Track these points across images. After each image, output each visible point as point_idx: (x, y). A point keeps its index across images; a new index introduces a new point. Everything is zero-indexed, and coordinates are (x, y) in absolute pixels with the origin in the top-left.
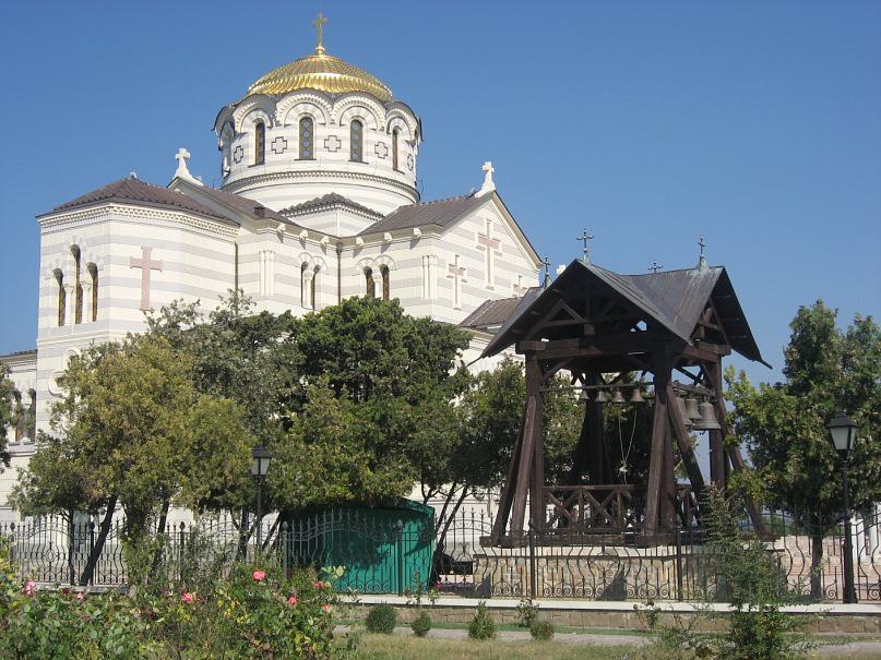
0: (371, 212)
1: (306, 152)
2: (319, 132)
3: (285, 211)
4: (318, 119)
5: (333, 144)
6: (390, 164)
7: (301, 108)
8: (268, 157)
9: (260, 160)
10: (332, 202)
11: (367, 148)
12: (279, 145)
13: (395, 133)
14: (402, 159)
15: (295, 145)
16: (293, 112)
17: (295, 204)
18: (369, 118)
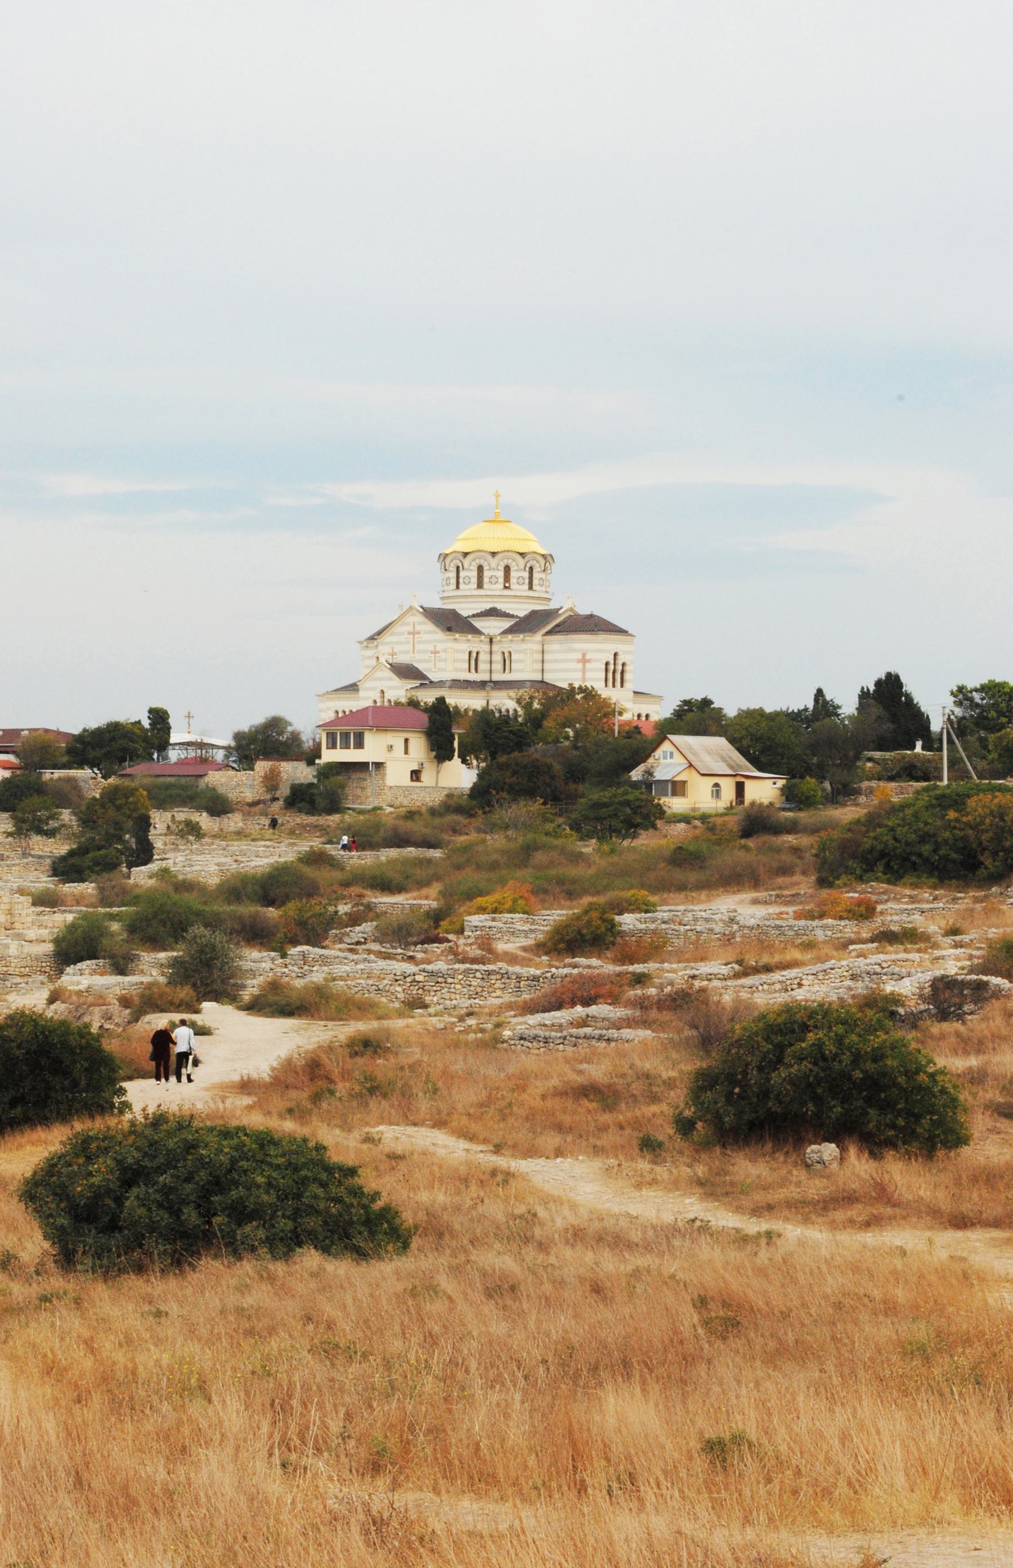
0: (512, 616)
1: (480, 585)
2: (487, 574)
3: (469, 617)
4: (486, 568)
5: (494, 580)
6: (526, 587)
7: (477, 561)
8: (461, 586)
9: (458, 587)
10: (493, 613)
11: (513, 580)
12: (467, 580)
13: (531, 569)
14: (535, 582)
15: (475, 580)
16: (473, 563)
17: (475, 612)
18: (514, 564)
